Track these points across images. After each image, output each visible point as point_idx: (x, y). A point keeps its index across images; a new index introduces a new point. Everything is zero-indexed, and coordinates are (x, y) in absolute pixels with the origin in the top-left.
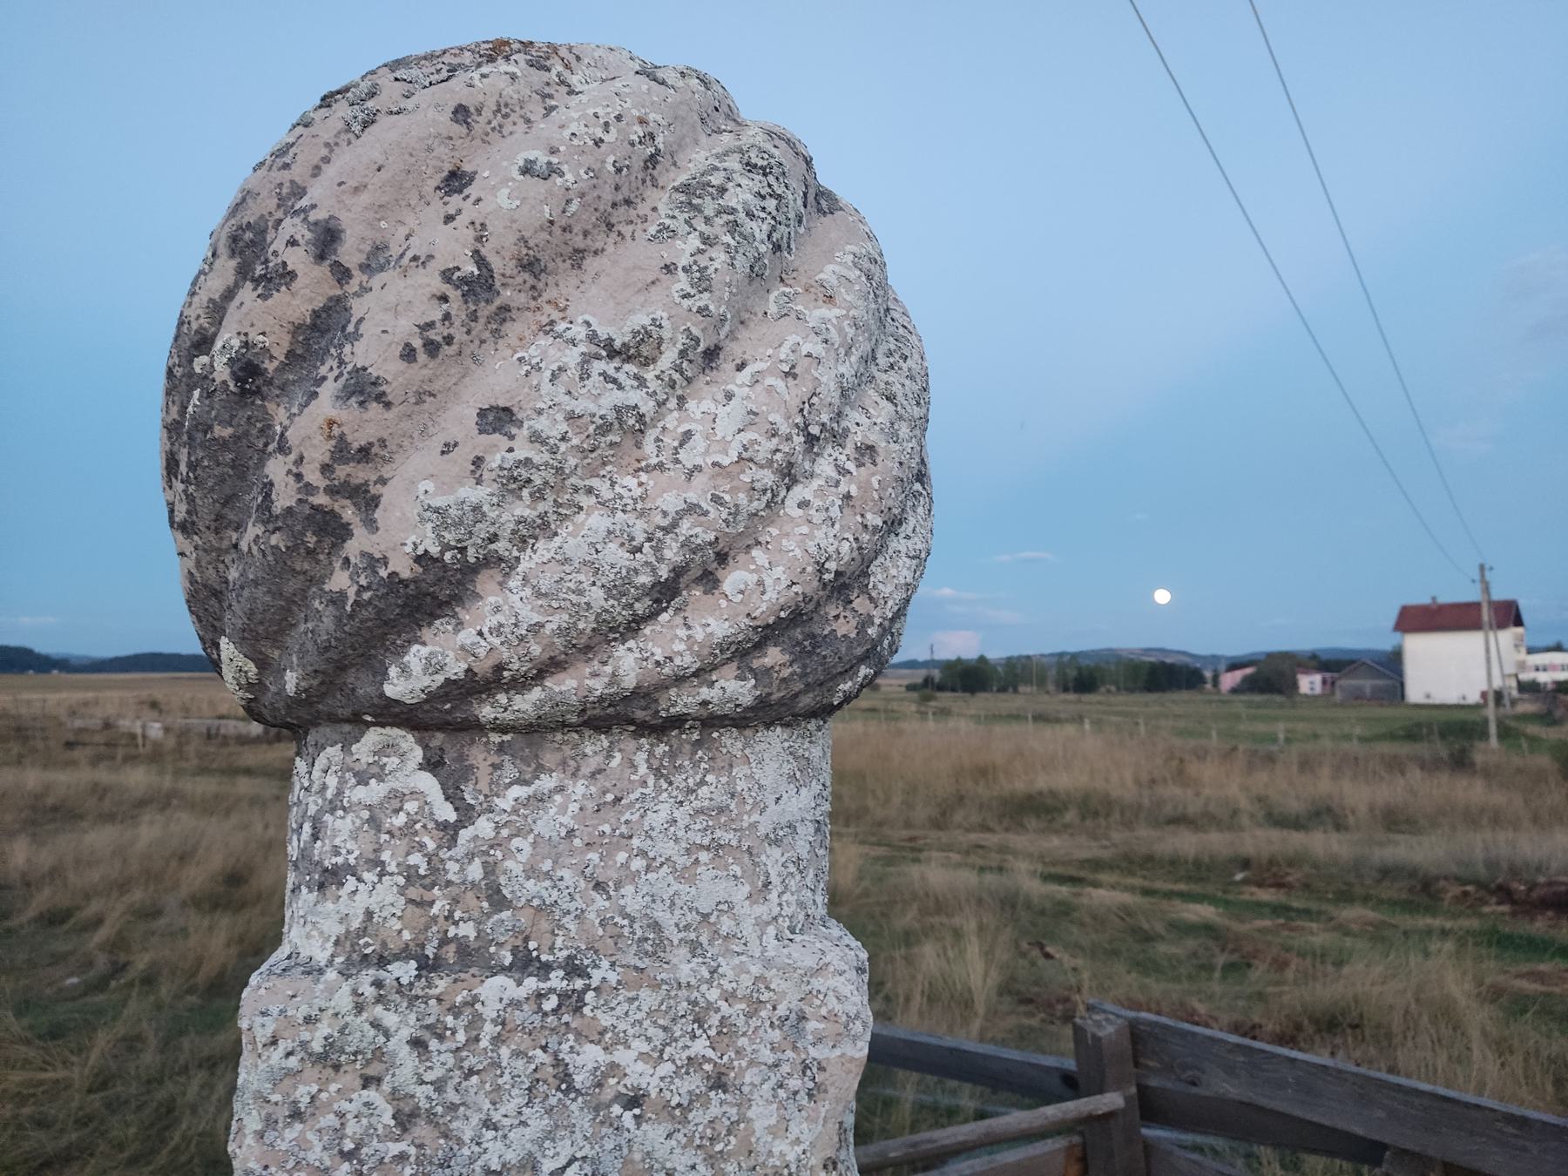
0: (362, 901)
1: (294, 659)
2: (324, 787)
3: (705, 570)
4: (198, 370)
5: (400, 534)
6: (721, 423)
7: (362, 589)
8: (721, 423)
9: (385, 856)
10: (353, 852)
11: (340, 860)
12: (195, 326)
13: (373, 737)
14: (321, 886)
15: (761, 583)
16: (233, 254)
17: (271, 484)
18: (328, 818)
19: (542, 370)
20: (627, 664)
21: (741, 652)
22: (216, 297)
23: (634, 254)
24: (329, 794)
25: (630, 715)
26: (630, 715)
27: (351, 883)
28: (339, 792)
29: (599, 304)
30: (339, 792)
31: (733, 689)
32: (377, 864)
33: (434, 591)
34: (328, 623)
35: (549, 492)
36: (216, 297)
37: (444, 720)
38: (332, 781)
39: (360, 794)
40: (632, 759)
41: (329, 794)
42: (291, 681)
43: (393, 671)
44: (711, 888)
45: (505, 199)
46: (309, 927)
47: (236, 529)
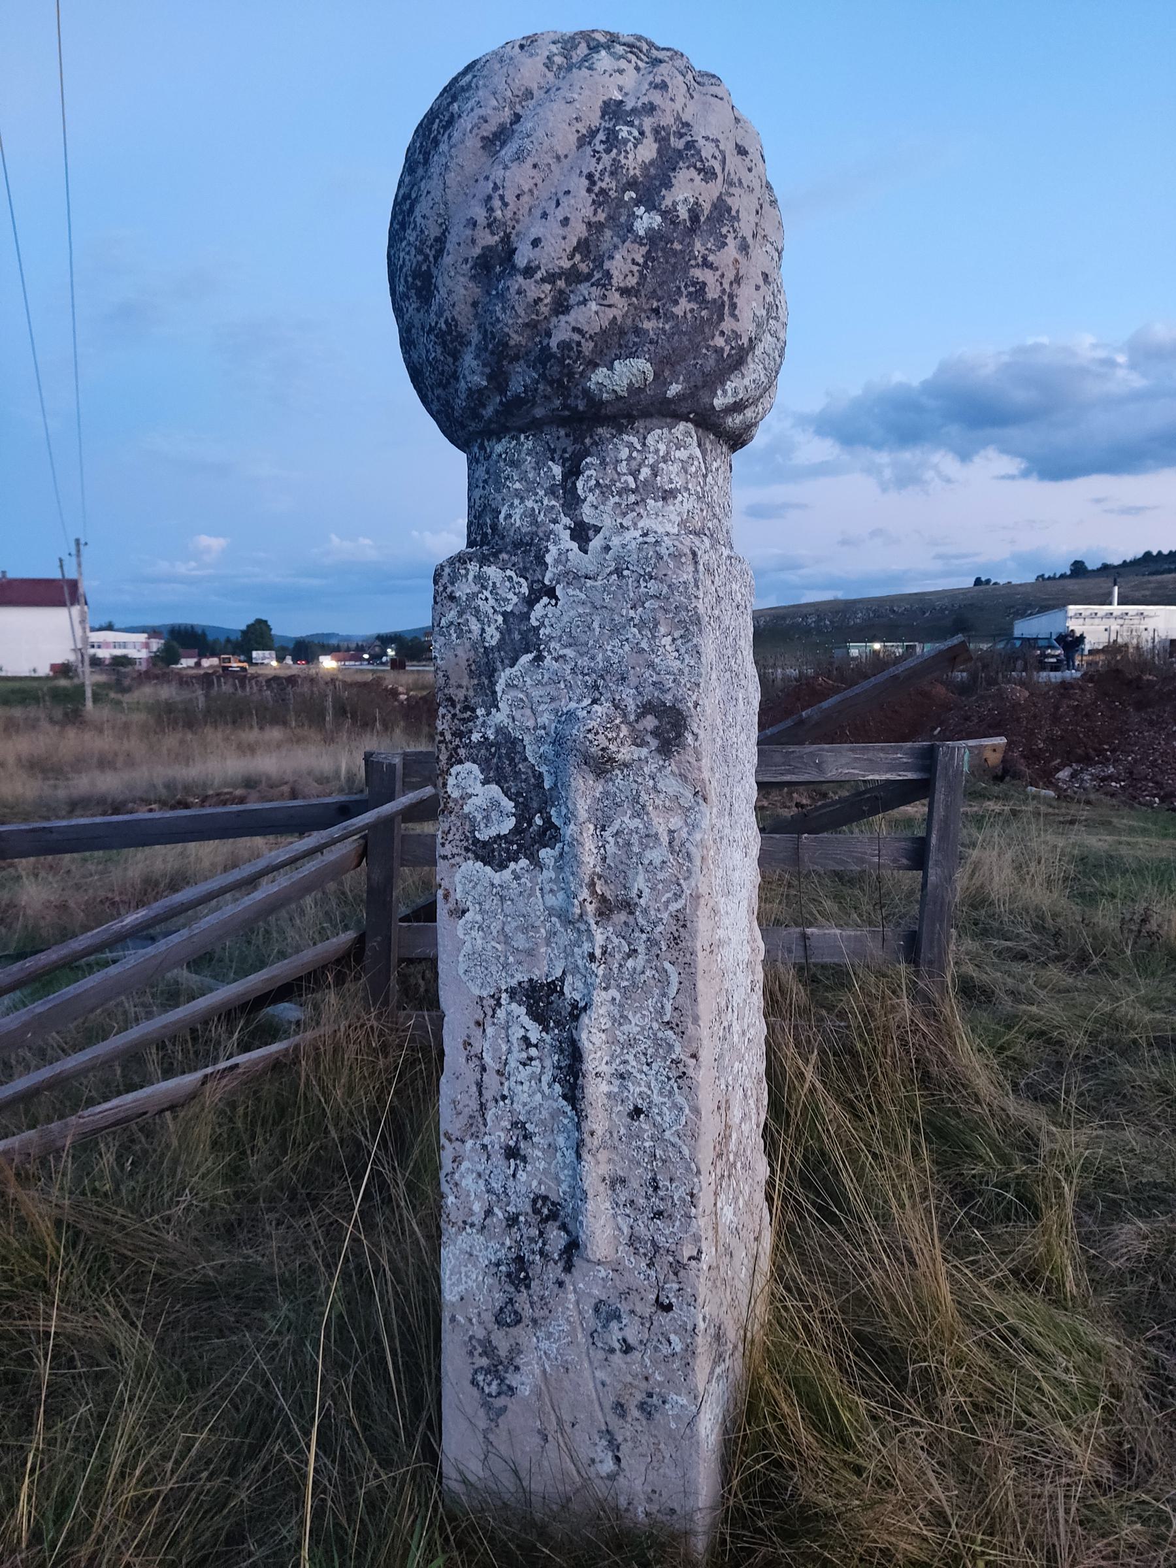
0: (687, 506)
1: (681, 378)
2: (657, 451)
4: (626, 198)
7: (732, 348)
9: (690, 486)
10: (679, 482)
11: (673, 486)
12: (632, 173)
13: (682, 426)
14: (664, 499)
16: (655, 141)
17: (705, 284)
18: (662, 465)
22: (647, 161)
24: (661, 454)
27: (680, 497)
28: (668, 453)
30: (668, 453)
32: (687, 489)
34: (712, 362)
36: (647, 161)
38: (662, 448)
39: (678, 454)
41: (661, 454)
42: (674, 389)
43: (719, 392)
46: (660, 518)
47: (658, 301)
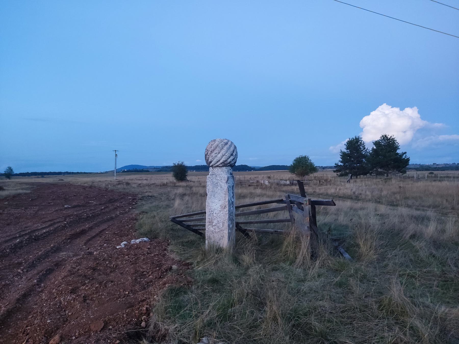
3: (219, 161)
5: (210, 160)
6: (219, 155)
8: (219, 155)
15: (221, 161)
19: (213, 154)
20: (217, 164)
21: (221, 163)
23: (216, 150)
25: (217, 166)
26: (217, 166)
29: (215, 152)
31: (221, 165)
33: (211, 162)
35: (214, 159)
37: (212, 166)
40: (219, 168)
44: (222, 173)
45: (212, 148)
